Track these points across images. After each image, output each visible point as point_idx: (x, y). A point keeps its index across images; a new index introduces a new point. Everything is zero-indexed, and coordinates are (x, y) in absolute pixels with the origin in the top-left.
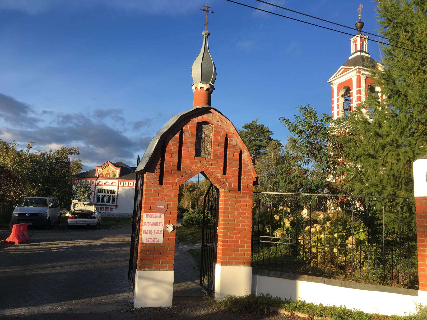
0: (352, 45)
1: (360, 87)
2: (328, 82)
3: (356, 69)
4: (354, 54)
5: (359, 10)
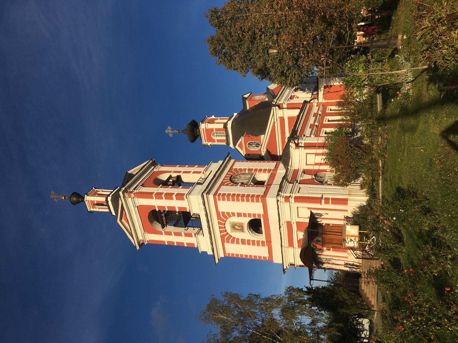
1: (152, 193)
2: (138, 248)
3: (124, 197)
4: (109, 208)
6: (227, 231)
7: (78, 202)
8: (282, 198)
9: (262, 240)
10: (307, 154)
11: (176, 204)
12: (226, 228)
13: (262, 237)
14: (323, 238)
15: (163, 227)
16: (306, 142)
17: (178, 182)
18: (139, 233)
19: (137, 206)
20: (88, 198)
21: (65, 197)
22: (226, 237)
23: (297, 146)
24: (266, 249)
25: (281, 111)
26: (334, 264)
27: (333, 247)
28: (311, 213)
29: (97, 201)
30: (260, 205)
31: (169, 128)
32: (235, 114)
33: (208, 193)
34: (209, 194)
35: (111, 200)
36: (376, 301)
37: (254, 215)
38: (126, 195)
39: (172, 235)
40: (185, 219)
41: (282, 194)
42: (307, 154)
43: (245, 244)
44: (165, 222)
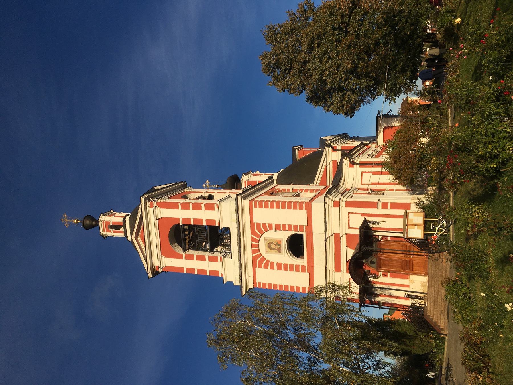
0: (111, 234)
2: (150, 276)
3: (145, 205)
5: (68, 223)
6: (261, 252)
7: (91, 227)
8: (330, 200)
9: (302, 264)
10: (362, 172)
11: (204, 216)
12: (260, 248)
13: (302, 262)
14: (379, 259)
15: (184, 251)
16: (362, 160)
17: (211, 197)
18: (156, 256)
19: (158, 219)
20: (104, 219)
21: (77, 220)
22: (258, 260)
23: (352, 164)
24: (306, 275)
25: (335, 153)
26: (391, 296)
27: (391, 272)
28: (365, 219)
29: (113, 222)
30: (303, 213)
31: (208, 181)
32: (282, 170)
33: (244, 198)
34: (245, 199)
35: (130, 219)
36: (446, 318)
37: (296, 227)
38: (148, 204)
39: (193, 259)
40: (213, 238)
41: (331, 197)
42: (362, 172)
43: (281, 269)
44: (187, 246)
